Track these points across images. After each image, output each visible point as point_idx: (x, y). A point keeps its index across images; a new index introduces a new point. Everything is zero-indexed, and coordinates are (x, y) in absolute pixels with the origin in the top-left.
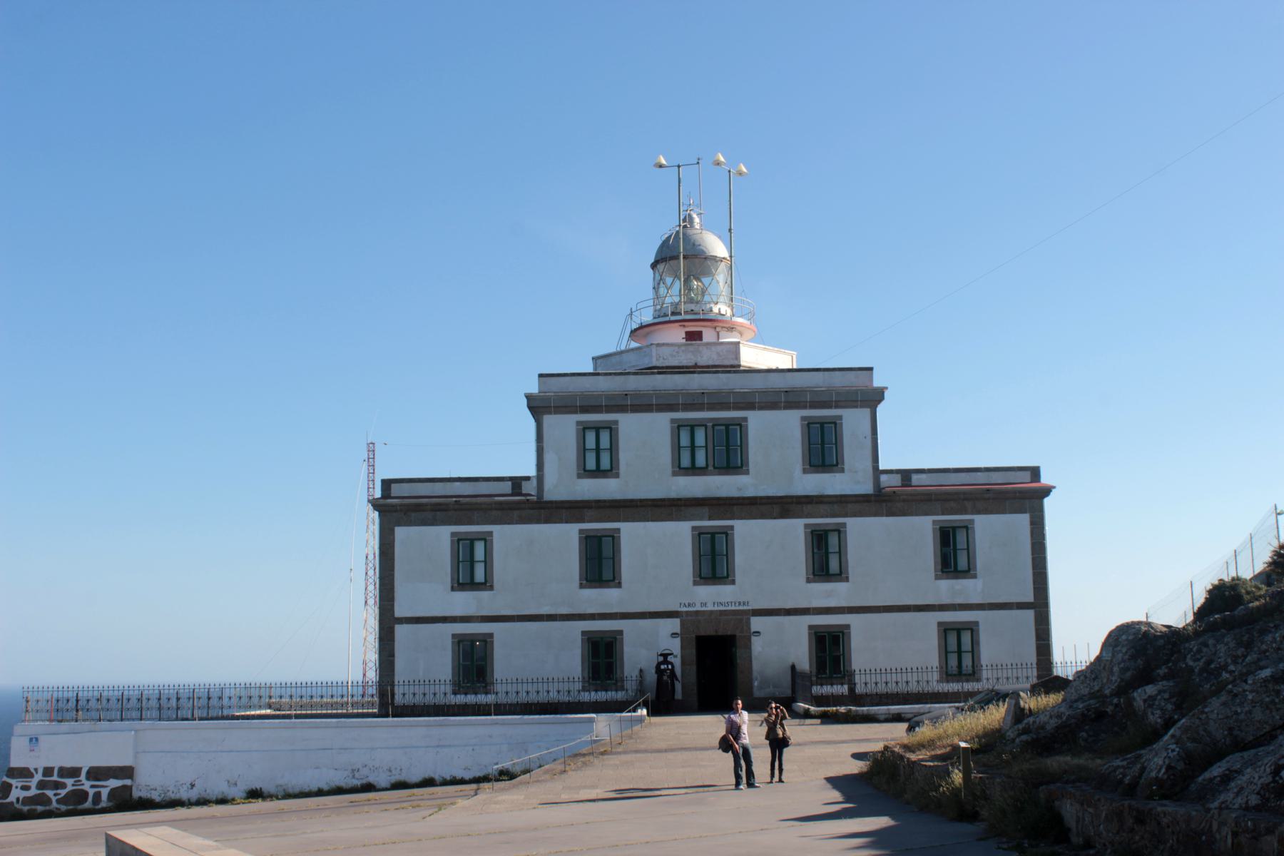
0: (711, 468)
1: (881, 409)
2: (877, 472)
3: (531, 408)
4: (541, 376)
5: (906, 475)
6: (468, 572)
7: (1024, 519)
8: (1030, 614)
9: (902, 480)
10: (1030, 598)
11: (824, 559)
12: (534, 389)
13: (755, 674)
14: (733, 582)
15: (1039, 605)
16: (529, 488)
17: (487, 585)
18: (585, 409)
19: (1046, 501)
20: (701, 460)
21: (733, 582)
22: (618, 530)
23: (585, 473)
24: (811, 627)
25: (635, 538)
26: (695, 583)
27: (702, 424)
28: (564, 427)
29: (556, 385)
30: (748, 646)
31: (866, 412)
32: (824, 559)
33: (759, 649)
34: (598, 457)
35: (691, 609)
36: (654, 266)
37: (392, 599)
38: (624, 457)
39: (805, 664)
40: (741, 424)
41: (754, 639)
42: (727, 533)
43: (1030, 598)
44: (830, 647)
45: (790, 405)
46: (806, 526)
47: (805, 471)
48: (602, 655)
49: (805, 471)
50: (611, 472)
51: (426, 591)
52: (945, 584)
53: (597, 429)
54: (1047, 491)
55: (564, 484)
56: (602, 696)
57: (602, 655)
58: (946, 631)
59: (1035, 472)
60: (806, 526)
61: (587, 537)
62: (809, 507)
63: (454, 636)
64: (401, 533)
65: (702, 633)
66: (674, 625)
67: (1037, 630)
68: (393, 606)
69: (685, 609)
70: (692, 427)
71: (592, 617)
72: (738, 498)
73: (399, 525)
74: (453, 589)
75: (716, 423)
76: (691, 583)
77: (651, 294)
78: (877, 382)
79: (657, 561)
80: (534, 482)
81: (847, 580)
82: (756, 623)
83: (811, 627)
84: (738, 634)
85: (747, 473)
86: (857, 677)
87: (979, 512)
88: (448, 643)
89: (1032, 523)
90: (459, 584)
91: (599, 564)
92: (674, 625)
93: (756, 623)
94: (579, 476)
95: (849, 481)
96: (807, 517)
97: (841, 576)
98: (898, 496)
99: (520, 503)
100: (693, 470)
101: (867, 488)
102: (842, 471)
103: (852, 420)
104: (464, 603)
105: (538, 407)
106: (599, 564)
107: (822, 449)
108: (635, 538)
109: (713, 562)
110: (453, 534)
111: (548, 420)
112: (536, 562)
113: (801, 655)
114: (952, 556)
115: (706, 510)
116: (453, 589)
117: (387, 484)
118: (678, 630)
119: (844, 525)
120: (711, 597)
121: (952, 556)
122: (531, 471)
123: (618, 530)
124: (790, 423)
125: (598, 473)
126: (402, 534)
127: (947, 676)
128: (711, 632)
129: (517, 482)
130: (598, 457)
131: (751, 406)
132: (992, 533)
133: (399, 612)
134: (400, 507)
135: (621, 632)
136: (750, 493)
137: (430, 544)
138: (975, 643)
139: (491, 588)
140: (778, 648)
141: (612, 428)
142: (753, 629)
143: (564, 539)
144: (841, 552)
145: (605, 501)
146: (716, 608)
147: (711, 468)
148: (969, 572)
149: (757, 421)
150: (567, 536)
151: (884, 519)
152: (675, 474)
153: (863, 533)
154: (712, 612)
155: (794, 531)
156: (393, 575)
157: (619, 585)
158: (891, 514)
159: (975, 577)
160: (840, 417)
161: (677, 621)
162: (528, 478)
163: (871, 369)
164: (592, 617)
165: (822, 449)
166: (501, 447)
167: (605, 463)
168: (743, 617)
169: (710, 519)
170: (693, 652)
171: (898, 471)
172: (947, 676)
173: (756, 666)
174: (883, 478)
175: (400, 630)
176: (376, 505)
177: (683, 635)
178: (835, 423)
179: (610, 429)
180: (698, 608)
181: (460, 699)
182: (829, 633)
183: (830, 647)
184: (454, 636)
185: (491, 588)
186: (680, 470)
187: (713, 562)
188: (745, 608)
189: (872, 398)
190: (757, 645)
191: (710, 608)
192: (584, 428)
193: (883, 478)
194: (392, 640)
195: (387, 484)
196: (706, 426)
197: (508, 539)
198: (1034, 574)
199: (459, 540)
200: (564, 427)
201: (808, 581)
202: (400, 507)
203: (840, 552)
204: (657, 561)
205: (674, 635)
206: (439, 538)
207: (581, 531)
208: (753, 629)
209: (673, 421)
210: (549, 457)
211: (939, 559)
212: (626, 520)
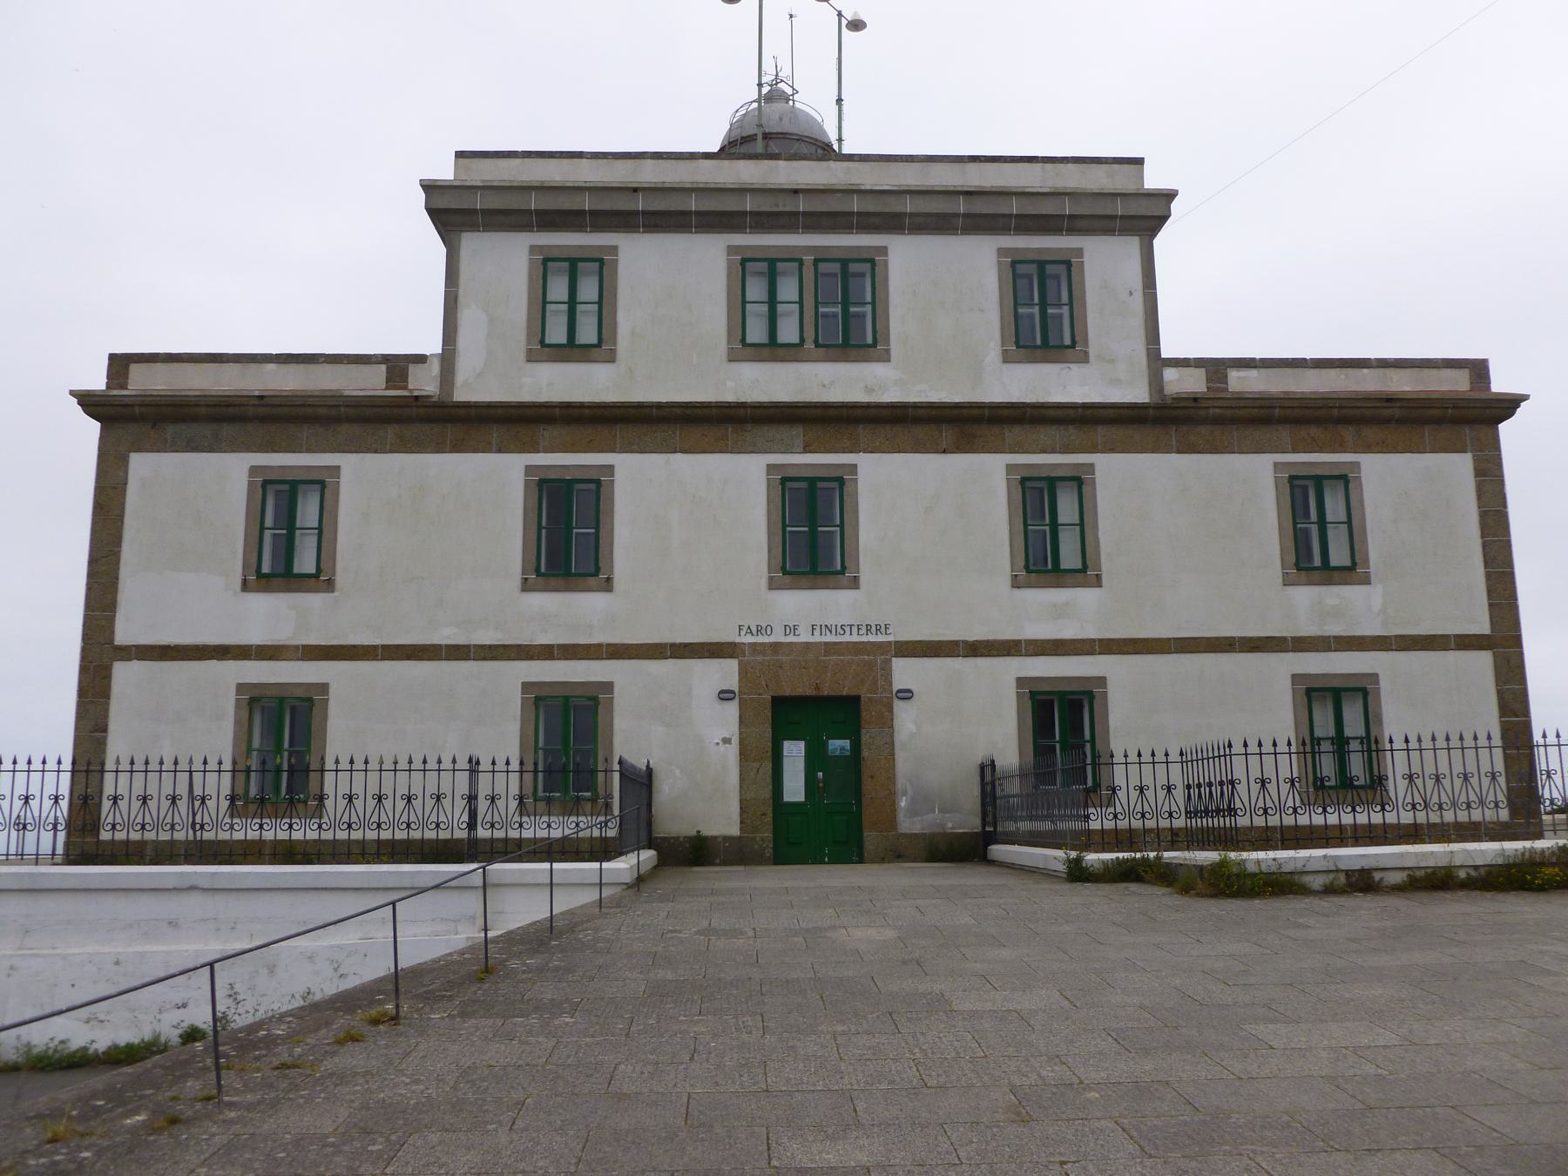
0: (809, 345)
2: (1157, 363)
3: (435, 213)
4: (460, 155)
5: (1216, 368)
6: (284, 551)
7: (1460, 466)
8: (1482, 663)
9: (1208, 380)
10: (1481, 624)
11: (1049, 542)
12: (445, 171)
13: (901, 782)
14: (855, 583)
15: (1503, 642)
16: (424, 383)
17: (321, 580)
19: (1504, 428)
20: (788, 332)
21: (855, 583)
22: (610, 469)
23: (543, 350)
24: (1021, 682)
25: (641, 483)
26: (773, 585)
27: (794, 258)
28: (505, 261)
30: (887, 721)
31: (1132, 244)
33: (912, 727)
34: (573, 314)
35: (761, 639)
37: (112, 606)
38: (627, 320)
40: (873, 262)
41: (898, 705)
42: (840, 482)
43: (1481, 624)
44: (1063, 722)
46: (1010, 468)
47: (1007, 358)
48: (567, 740)
49: (1007, 358)
50: (601, 349)
51: (194, 589)
52: (1305, 596)
53: (573, 264)
54: (1509, 405)
55: (496, 373)
56: (560, 828)
57: (567, 740)
58: (1309, 692)
59: (1478, 370)
60: (1010, 468)
61: (541, 482)
62: (1017, 429)
63: (241, 688)
64: (141, 465)
65: (787, 692)
66: (726, 673)
67: (1500, 693)
68: (112, 619)
69: (749, 639)
70: (772, 267)
71: (547, 652)
72: (868, 406)
73: (139, 450)
74: (245, 586)
76: (764, 582)
79: (688, 528)
80: (435, 367)
81: (1097, 581)
82: (904, 672)
83: (1021, 682)
84: (865, 694)
85: (885, 357)
86: (1238, 763)
87: (1368, 448)
88: (229, 703)
89: (1480, 472)
90: (260, 575)
91: (567, 538)
92: (726, 673)
93: (904, 672)
94: (532, 357)
96: (1013, 450)
97: (1086, 574)
99: (401, 411)
100: (773, 350)
101: (1138, 393)
102: (1084, 359)
103: (1104, 261)
104: (271, 617)
107: (1043, 315)
109: (812, 537)
110: (254, 470)
111: (471, 242)
112: (430, 537)
113: (1002, 738)
114: (1318, 540)
115: (797, 433)
116: (245, 586)
117: (120, 364)
118: (733, 684)
119: (1091, 467)
120: (808, 615)
121: (1318, 540)
122: (432, 344)
123: (610, 469)
124: (976, 263)
125: (572, 351)
127: (1319, 790)
129: (398, 366)
130: (573, 314)
131: (894, 223)
132: (1398, 488)
133: (126, 632)
135: (608, 687)
136: (892, 395)
138: (1370, 718)
139: (330, 585)
140: (955, 729)
141: (603, 264)
142: (897, 686)
144: (1085, 525)
145: (581, 406)
146: (817, 638)
147: (809, 345)
148: (1353, 572)
149: (909, 261)
150: (499, 481)
151: (1174, 456)
152: (733, 358)
153: (1133, 490)
154: (807, 645)
155: (984, 479)
156: (117, 555)
157: (608, 586)
159: (1366, 580)
160: (1079, 252)
161: (732, 665)
162: (420, 359)
163: (1139, 162)
164: (547, 652)
165: (1043, 315)
167: (587, 334)
168: (877, 656)
169: (807, 449)
171: (1199, 363)
172: (1319, 790)
173: (903, 764)
174: (1170, 374)
175: (124, 674)
176: (89, 402)
177: (740, 696)
178: (1069, 265)
179: (601, 261)
180: (778, 637)
181: (246, 831)
182: (1062, 694)
183: (1063, 722)
184: (241, 688)
185: (330, 585)
186: (743, 349)
187: (812, 537)
188: (881, 638)
189: (1142, 215)
190: (906, 719)
191: (804, 637)
192: (545, 263)
193: (1170, 374)
194: (106, 694)
195: (120, 364)
196: (801, 262)
197: (372, 488)
198: (1488, 576)
199: (265, 483)
201: (1016, 583)
203: (1082, 524)
204: (688, 528)
205: (725, 696)
206: (222, 480)
207: (529, 469)
208: (897, 686)
209: (731, 250)
210: (469, 316)
211: (1291, 543)
212: (628, 448)
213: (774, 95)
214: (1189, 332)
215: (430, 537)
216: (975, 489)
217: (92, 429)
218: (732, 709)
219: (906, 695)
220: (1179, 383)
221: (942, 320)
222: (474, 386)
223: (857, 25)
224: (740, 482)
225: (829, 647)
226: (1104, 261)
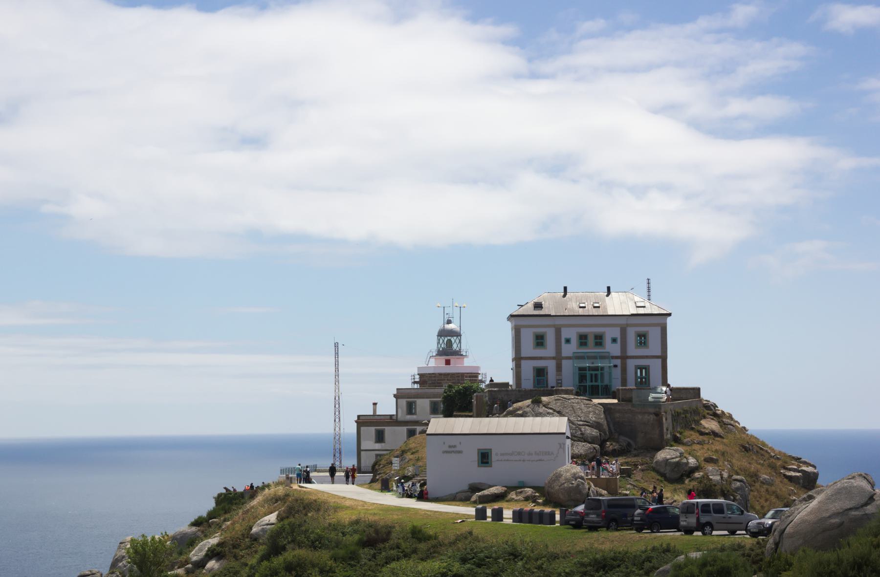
6: (380, 437)
12: (395, 393)
16: (394, 418)
55: (403, 416)
64: (362, 428)
99: (391, 421)
117: (359, 416)
129: (391, 416)
130: (411, 408)
143: (404, 430)
150: (404, 430)
166: (388, 407)
175: (362, 453)
195: (359, 416)
197: (388, 430)
200: (403, 402)
206: (372, 430)
210: (399, 410)
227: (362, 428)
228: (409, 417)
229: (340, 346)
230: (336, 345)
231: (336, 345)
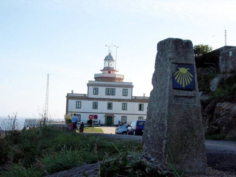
1: (133, 88)
2: (132, 96)
11: (124, 108)
12: (88, 83)
16: (87, 96)
18: (95, 86)
20: (109, 93)
25: (100, 103)
27: (110, 89)
28: (92, 88)
29: (91, 82)
31: (131, 88)
32: (124, 108)
34: (96, 92)
36: (104, 60)
39: (121, 121)
40: (115, 89)
41: (114, 117)
45: (121, 87)
55: (92, 96)
64: (69, 100)
66: (104, 115)
70: (108, 89)
75: (112, 89)
77: (104, 64)
78: (133, 85)
79: (103, 107)
84: (113, 116)
87: (145, 102)
91: (95, 106)
93: (115, 115)
95: (128, 97)
98: (135, 100)
99: (85, 97)
101: (130, 98)
103: (129, 89)
105: (88, 85)
106: (95, 106)
107: (125, 93)
108: (100, 103)
109: (110, 106)
111: (90, 87)
112: (87, 106)
115: (109, 100)
120: (109, 111)
122: (87, 94)
124: (121, 89)
126: (70, 101)
128: (109, 116)
129: (85, 95)
130: (96, 92)
134: (70, 97)
137: (73, 102)
140: (117, 119)
153: (129, 104)
158: (133, 102)
165: (125, 93)
166: (83, 90)
168: (113, 114)
170: (106, 118)
187: (110, 106)
195: (68, 94)
200: (92, 88)
202: (70, 97)
204: (103, 107)
213: (110, 54)
214: (134, 94)
215: (87, 106)
216: (120, 104)
217: (66, 98)
218: (105, 117)
219: (115, 117)
220: (133, 98)
221: (119, 93)
222: (90, 97)
223: (118, 47)
224: (105, 103)
225: (110, 113)
226: (129, 89)
227: (69, 100)
228: (94, 96)
229: (50, 75)
230: (48, 75)
231: (48, 75)
